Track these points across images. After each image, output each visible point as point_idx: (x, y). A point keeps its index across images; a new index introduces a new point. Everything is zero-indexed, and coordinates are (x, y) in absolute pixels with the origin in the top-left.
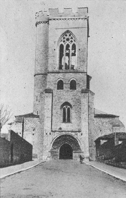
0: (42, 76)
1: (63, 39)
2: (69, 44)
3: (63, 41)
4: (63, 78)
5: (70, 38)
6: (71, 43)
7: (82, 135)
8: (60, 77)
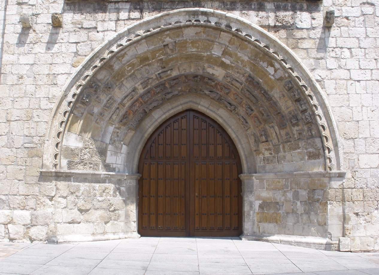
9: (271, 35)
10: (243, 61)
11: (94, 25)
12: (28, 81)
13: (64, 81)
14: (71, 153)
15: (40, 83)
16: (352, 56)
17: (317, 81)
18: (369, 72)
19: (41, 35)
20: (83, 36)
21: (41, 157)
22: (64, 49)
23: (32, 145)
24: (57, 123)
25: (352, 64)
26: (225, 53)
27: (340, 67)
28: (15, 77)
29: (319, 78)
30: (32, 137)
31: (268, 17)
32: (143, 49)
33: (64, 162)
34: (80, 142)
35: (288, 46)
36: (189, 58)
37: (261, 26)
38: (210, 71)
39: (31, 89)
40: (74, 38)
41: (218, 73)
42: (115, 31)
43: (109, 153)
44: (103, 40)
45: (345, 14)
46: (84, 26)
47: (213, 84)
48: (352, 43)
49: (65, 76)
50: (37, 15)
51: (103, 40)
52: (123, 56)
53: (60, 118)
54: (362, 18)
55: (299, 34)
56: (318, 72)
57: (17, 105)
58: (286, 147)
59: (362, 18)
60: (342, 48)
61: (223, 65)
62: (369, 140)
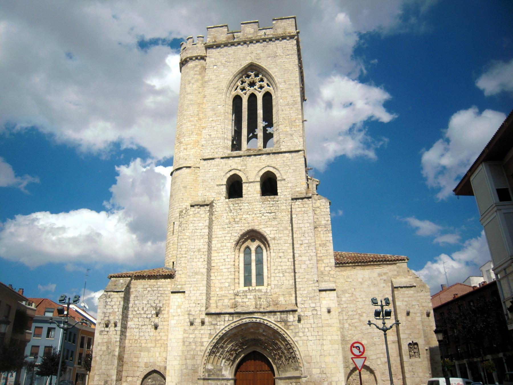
0: (188, 170)
1: (242, 84)
2: (256, 93)
3: (241, 89)
4: (239, 168)
5: (257, 81)
6: (259, 90)
7: (299, 320)
8: (233, 167)
9: (279, 324)
10: (270, 334)
11: (216, 323)
12: (193, 344)
13: (206, 344)
14: (209, 371)
15: (197, 345)
16: (308, 331)
17: (296, 341)
18: (315, 337)
20: (212, 327)
21: (198, 373)
22: (206, 332)
23: (195, 368)
24: (204, 360)
25: (309, 334)
26: (264, 331)
27: (304, 336)
28: (188, 343)
29: (296, 340)
30: (195, 365)
31: (277, 318)
32: (234, 331)
33: (207, 374)
34: (212, 366)
35: (285, 328)
36: (252, 333)
37: (276, 321)
38: (260, 337)
39: (194, 347)
40: (209, 328)
41: (263, 338)
42: (224, 325)
43: (223, 370)
44: (220, 329)
45: (306, 315)
46: (213, 323)
47: (261, 342)
48: (309, 326)
49: (206, 342)
50: (195, 319)
51: (220, 329)
52: (227, 334)
53: (205, 358)
54: (312, 316)
55: (289, 324)
56: (296, 338)
57: (189, 353)
58: (288, 366)
59: (312, 316)
60: (305, 328)
61: (264, 335)
62: (316, 363)
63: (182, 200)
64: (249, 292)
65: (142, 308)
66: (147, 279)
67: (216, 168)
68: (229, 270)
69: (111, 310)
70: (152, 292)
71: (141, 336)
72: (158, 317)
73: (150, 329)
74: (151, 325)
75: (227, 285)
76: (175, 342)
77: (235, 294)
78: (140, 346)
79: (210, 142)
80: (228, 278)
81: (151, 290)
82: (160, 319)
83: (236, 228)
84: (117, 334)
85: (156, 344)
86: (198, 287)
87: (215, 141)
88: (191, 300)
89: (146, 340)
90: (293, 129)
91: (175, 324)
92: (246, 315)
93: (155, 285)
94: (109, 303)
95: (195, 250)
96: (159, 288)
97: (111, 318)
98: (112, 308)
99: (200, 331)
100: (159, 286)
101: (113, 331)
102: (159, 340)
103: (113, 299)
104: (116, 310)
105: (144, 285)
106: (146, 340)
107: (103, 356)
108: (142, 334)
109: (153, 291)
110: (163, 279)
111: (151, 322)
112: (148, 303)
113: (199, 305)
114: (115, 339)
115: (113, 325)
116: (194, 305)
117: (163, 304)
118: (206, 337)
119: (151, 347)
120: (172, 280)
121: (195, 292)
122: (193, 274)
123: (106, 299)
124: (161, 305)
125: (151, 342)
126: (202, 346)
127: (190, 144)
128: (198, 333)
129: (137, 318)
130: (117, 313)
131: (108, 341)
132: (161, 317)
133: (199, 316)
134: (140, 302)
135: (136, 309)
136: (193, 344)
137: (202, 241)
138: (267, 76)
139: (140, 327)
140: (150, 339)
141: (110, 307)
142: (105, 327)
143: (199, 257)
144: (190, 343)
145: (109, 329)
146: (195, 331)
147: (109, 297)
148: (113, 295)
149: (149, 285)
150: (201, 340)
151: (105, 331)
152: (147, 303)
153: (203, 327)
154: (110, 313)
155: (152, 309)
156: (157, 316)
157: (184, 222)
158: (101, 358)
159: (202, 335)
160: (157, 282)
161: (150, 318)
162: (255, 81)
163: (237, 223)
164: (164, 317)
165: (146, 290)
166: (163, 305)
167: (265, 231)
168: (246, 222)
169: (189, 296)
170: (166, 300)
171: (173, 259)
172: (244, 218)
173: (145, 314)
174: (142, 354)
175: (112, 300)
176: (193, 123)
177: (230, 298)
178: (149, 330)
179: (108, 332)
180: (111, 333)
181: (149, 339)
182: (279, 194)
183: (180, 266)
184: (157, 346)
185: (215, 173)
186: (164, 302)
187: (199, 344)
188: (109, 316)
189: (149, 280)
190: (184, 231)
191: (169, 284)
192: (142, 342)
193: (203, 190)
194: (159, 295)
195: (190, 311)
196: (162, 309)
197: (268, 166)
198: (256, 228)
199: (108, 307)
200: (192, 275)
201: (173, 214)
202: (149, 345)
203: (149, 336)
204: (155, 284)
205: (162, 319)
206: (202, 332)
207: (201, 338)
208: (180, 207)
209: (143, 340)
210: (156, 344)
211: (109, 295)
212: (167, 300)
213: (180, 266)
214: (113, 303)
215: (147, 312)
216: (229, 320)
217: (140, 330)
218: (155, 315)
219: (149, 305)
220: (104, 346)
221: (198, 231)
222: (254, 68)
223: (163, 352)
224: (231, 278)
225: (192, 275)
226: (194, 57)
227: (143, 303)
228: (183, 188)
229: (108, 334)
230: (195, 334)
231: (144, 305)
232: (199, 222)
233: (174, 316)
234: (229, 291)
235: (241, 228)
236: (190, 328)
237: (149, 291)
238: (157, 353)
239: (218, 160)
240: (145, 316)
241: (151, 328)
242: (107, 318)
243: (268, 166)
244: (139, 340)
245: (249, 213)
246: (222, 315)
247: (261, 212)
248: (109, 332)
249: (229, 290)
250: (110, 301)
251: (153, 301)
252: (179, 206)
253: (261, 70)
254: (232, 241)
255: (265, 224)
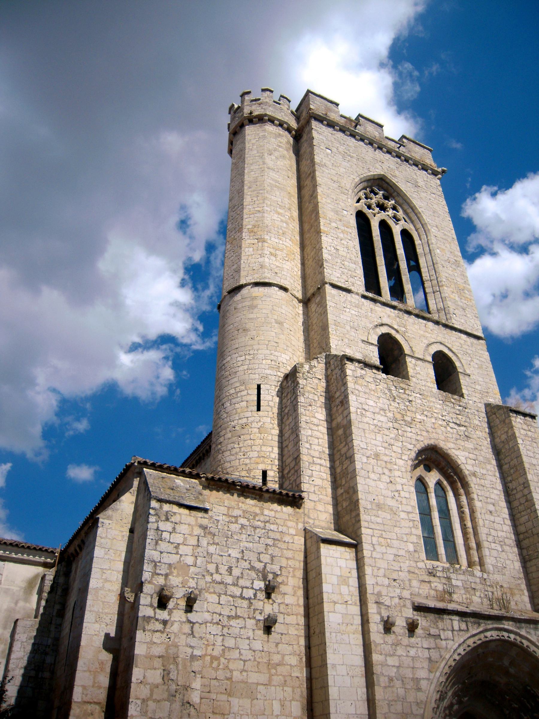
0: (281, 293)
19: (400, 637)
22: (420, 654)
39: (401, 691)
63: (276, 345)
64: (454, 572)
65: (226, 567)
66: (236, 495)
67: (355, 309)
68: (410, 515)
69: (174, 559)
70: (250, 531)
71: (229, 648)
72: (270, 601)
73: (254, 630)
74: (255, 618)
75: (411, 548)
76: (346, 674)
77: (430, 571)
78: (228, 679)
79: (339, 261)
80: (411, 534)
81: (247, 523)
82: (276, 606)
83: (409, 435)
84: (195, 634)
85: (271, 675)
86: (389, 540)
87: (346, 263)
88: (379, 569)
89: (242, 662)
90: (462, 300)
91: (339, 624)
92: (489, 622)
93: (256, 515)
94: (165, 535)
95: (370, 452)
96: (267, 524)
97: (175, 580)
98: (177, 553)
99: (409, 648)
100: (268, 518)
101: (182, 623)
102: (278, 665)
103: (177, 526)
104: (190, 560)
105: (229, 508)
106: (245, 661)
107: (150, 703)
108: (230, 642)
109: (255, 528)
110: (276, 505)
111: (254, 613)
112: (242, 559)
113: (395, 584)
114: (189, 650)
115: (183, 604)
116: (386, 582)
117: (281, 567)
118: (423, 668)
119: (258, 684)
120: (298, 510)
121: (383, 549)
122: (374, 508)
123: (157, 522)
124: (275, 568)
125: (257, 670)
126: (419, 689)
127: (282, 250)
128: (404, 654)
129: (214, 593)
130: (192, 569)
131: (167, 651)
132: (279, 601)
133: (401, 612)
134: (222, 551)
135: (212, 568)
136: (398, 684)
137: (379, 437)
138: (406, 207)
139: (225, 621)
140: (255, 660)
141: (171, 548)
142: (156, 605)
143: (380, 470)
144: (391, 680)
145: (170, 614)
146: (398, 648)
147: (167, 519)
148: (178, 516)
149: (244, 511)
150: (413, 674)
151: (157, 620)
152: (239, 556)
153: (413, 640)
154: (170, 565)
155: (253, 574)
156: (268, 596)
157: (309, 388)
158: (147, 712)
159: (413, 660)
160: (262, 509)
161: (249, 599)
162: (385, 205)
163: (409, 424)
164: (286, 602)
165: (236, 522)
166: (280, 570)
167: (457, 456)
168: (424, 429)
169: (371, 557)
170: (287, 558)
171: (263, 462)
172: (419, 421)
173: (237, 585)
174: (235, 701)
175: (174, 528)
176: (282, 218)
177: (421, 578)
178: (251, 634)
179: (165, 623)
180: (175, 628)
181: (252, 658)
182: (465, 396)
183: (311, 482)
184: (274, 683)
185: (355, 317)
186: (284, 563)
187: (410, 685)
188: (167, 575)
189: (242, 499)
190: (310, 408)
191: (291, 518)
192: (231, 666)
193: (339, 340)
194: (270, 542)
195: (379, 594)
196: (279, 579)
197: (441, 343)
198: (442, 445)
199: (163, 546)
200: (372, 509)
201: (256, 366)
202: (254, 678)
203: (250, 649)
204: (257, 511)
205: (282, 606)
206: (412, 652)
207: (413, 668)
208: (272, 357)
209: (235, 659)
210: (271, 675)
211: (167, 512)
212: (290, 559)
213: (311, 482)
214: (177, 538)
215: (242, 582)
216: (460, 630)
217: (226, 630)
218: (264, 593)
219: (246, 565)
220: (155, 669)
221: (368, 414)
222: (385, 185)
223: (291, 701)
224: (416, 535)
225: (372, 509)
226: (278, 120)
227: (229, 555)
228: (276, 323)
229: (167, 630)
230: (399, 656)
231: (234, 560)
232: (367, 396)
233: (335, 603)
234: (417, 562)
235: (419, 438)
236: (386, 640)
237: (243, 526)
238: (274, 702)
239: (357, 297)
240: (237, 591)
241: (255, 628)
242: (161, 581)
243: (441, 343)
244: (222, 660)
245: (425, 413)
246: (445, 616)
247: (444, 418)
248: (168, 626)
249: (416, 560)
250: (170, 529)
251: (257, 555)
252: (271, 354)
253: (395, 194)
254: (405, 457)
255: (455, 442)
